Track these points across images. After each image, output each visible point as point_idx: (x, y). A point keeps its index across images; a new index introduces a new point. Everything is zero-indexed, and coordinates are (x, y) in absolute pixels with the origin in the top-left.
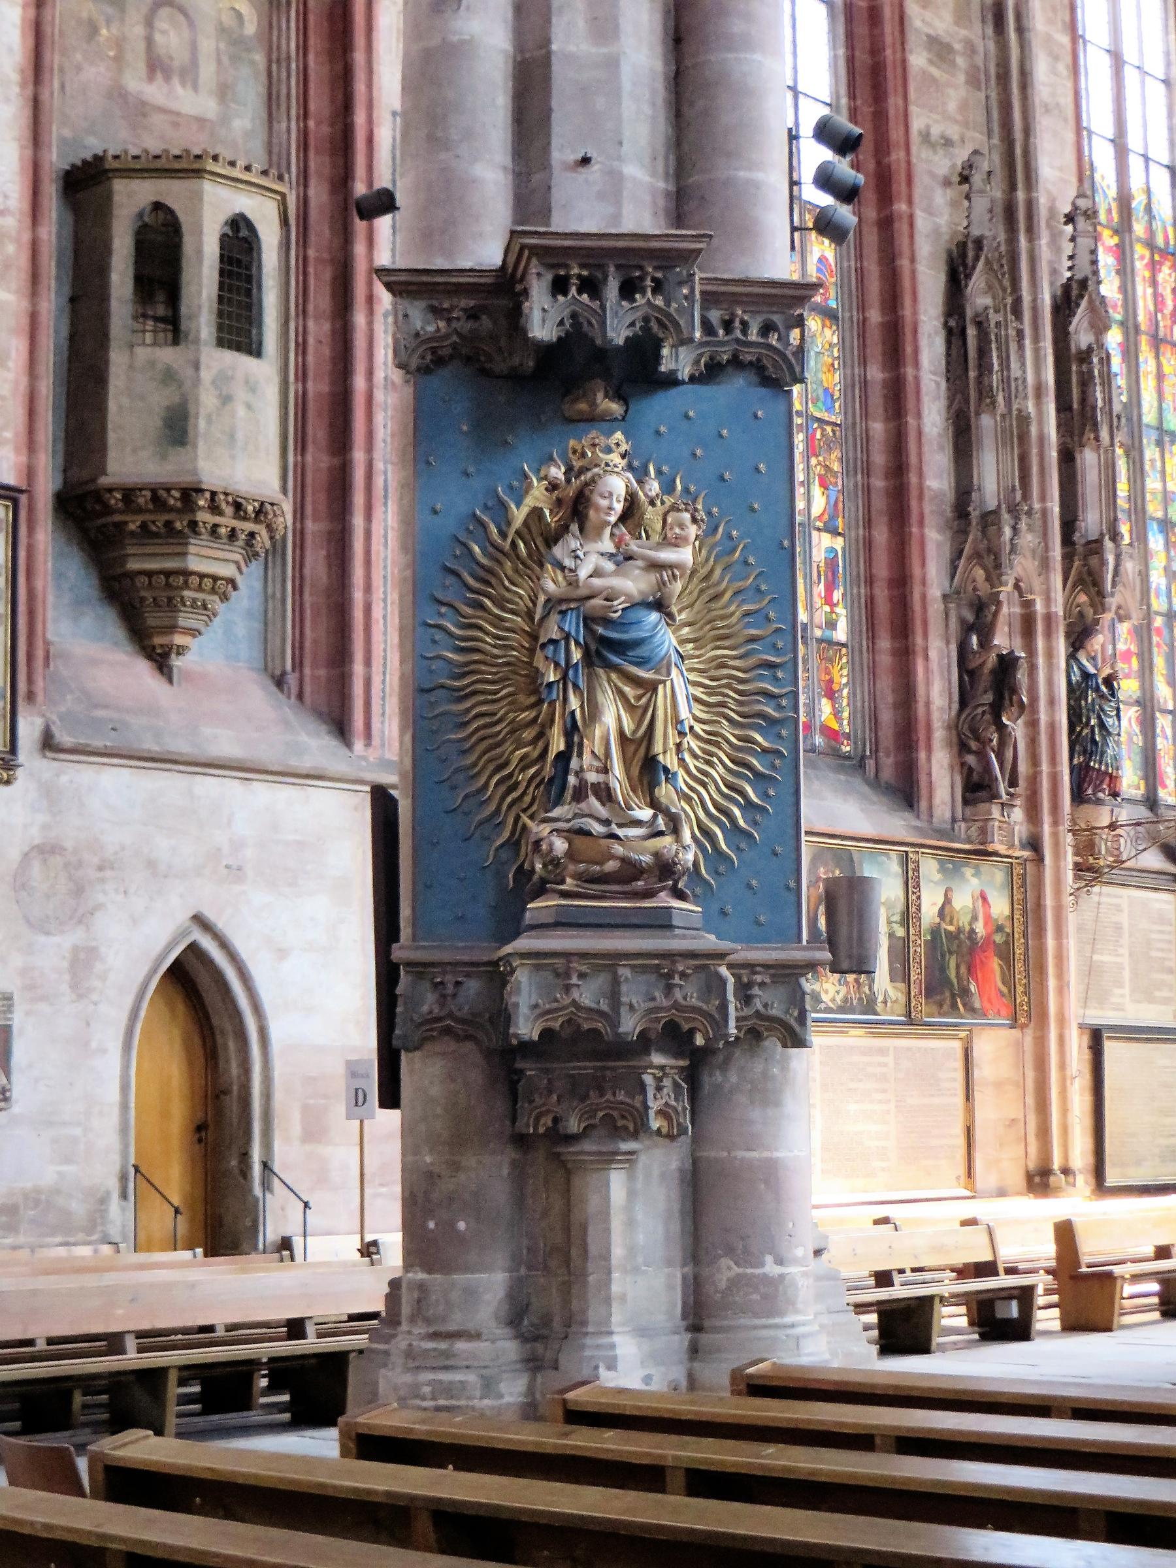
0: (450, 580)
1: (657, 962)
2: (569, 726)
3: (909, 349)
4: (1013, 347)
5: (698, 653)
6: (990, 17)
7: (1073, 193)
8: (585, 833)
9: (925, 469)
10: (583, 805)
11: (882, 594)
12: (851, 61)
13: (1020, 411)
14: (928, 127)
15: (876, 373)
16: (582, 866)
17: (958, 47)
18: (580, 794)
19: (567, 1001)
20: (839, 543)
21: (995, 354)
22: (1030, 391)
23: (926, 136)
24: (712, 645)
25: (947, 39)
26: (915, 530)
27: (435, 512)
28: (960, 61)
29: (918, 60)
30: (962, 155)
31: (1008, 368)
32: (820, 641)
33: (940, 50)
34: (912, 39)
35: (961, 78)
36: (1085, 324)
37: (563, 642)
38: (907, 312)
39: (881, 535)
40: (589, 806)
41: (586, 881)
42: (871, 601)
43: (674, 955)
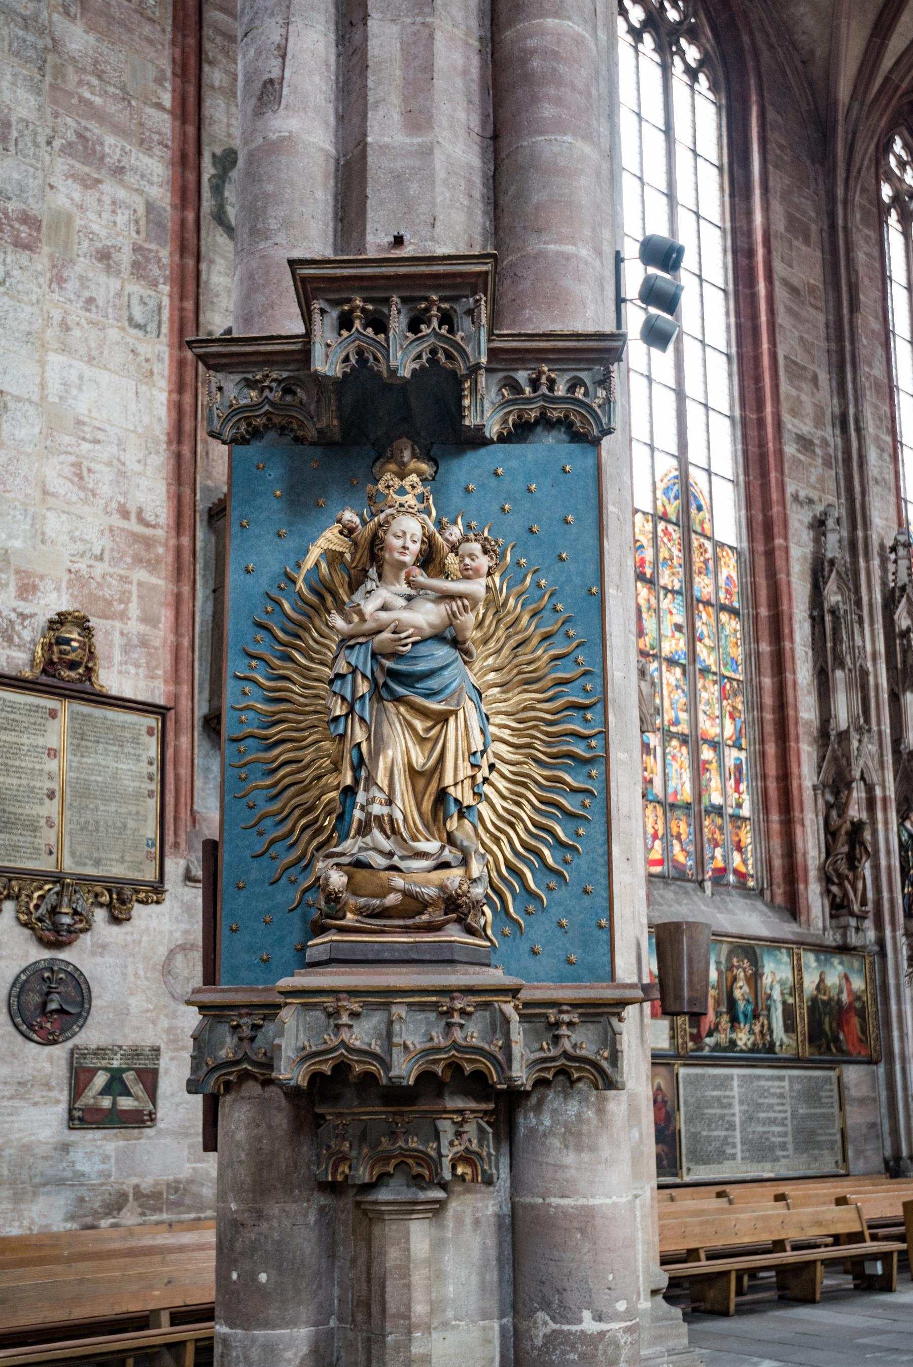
0: (261, 635)
1: (434, 999)
2: (355, 761)
3: (786, 631)
4: (856, 627)
6: (838, 423)
7: (894, 533)
8: (360, 864)
9: (799, 706)
10: (368, 839)
11: (772, 785)
12: (745, 452)
13: (861, 666)
14: (797, 491)
15: (765, 647)
16: (362, 901)
17: (817, 442)
18: (364, 829)
19: (335, 1042)
20: (743, 755)
21: (844, 631)
22: (869, 657)
23: (796, 498)
25: (808, 437)
26: (793, 744)
27: (248, 571)
28: (818, 451)
29: (790, 449)
30: (819, 508)
31: (853, 640)
32: (731, 816)
33: (805, 443)
34: (786, 437)
35: (820, 461)
36: (905, 614)
37: (350, 677)
38: (785, 607)
39: (771, 749)
40: (373, 840)
41: (368, 916)
42: (765, 791)
43: (452, 991)
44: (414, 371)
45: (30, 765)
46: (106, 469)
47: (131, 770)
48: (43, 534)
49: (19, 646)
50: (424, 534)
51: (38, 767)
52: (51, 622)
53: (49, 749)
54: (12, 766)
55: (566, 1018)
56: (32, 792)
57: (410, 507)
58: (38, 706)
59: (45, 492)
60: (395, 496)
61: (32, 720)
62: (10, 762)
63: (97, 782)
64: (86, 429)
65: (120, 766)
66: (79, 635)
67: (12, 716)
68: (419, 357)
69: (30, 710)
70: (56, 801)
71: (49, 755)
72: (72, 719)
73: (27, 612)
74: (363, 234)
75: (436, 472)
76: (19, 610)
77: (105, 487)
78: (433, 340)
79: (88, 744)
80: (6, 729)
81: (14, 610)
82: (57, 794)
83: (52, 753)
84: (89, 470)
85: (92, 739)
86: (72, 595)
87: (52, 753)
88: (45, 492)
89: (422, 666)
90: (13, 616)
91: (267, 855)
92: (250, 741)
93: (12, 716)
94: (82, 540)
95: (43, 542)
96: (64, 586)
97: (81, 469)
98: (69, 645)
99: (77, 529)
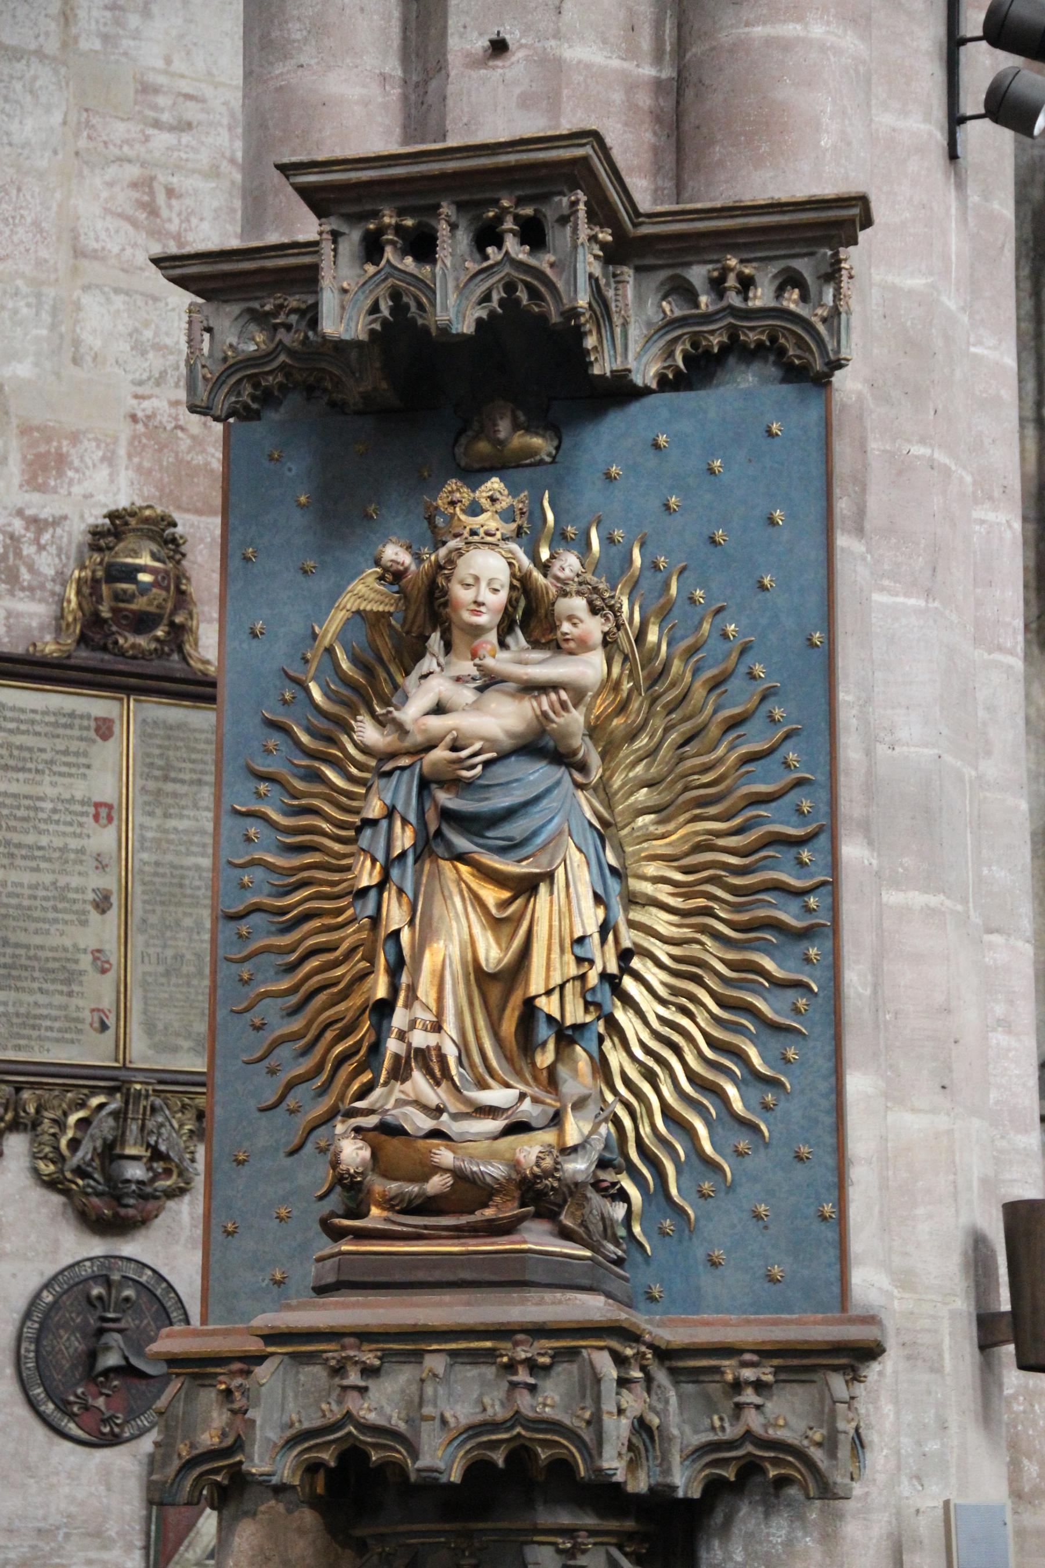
5: (661, 829)
24: (687, 816)
44: (479, 321)
45: (58, 842)
46: (205, 186)
48: (76, 343)
49: (31, 589)
50: (513, 575)
51: (74, 843)
52: (96, 533)
53: (97, 805)
54: (19, 846)
55: (748, 1374)
56: (64, 899)
57: (488, 534)
58: (72, 715)
59: (78, 252)
60: (463, 517)
62: (16, 838)
64: (162, 101)
66: (154, 557)
67: (18, 740)
68: (486, 298)
69: (56, 724)
70: (114, 914)
71: (96, 817)
72: (145, 736)
73: (45, 514)
74: (443, 35)
75: (558, 448)
76: (29, 512)
77: (206, 226)
78: (507, 269)
80: (6, 768)
81: (20, 513)
82: (114, 899)
83: (104, 813)
84: (170, 192)
85: (187, 776)
86: (139, 469)
87: (103, 812)
88: (78, 252)
89: (501, 801)
91: (284, 1105)
92: (256, 918)
93: (18, 740)
94: (157, 347)
95: (76, 361)
96: (122, 452)
97: (152, 193)
98: (134, 580)
99: (147, 324)
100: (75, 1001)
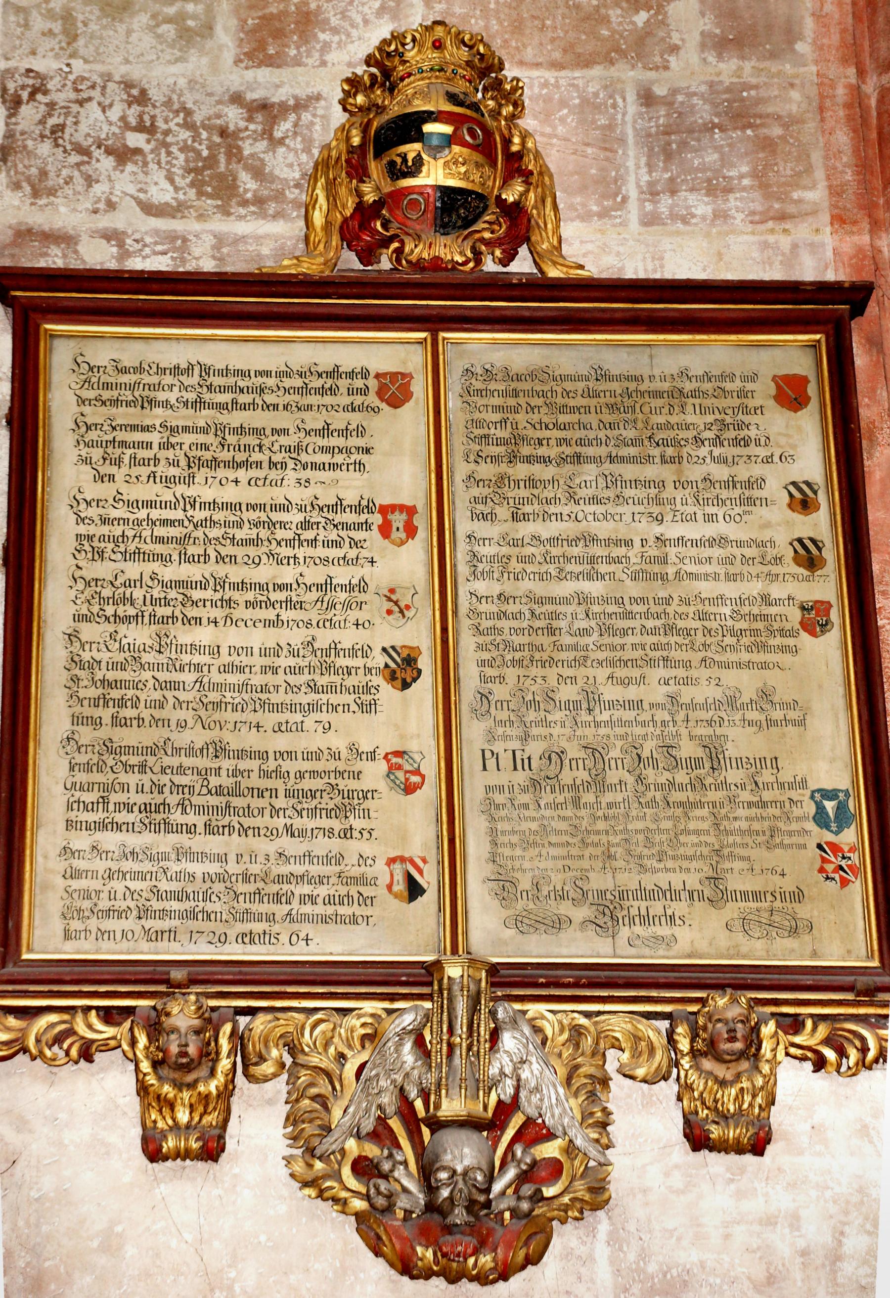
47: (722, 541)
49: (259, 201)
51: (342, 575)
53: (385, 510)
54: (241, 586)
56: (329, 668)
58: (335, 373)
61: (314, 421)
62: (235, 574)
63: (583, 599)
65: (673, 531)
67: (236, 418)
69: (304, 390)
71: (385, 530)
76: (250, 96)
79: (538, 471)
80: (215, 463)
81: (237, 99)
82: (425, 663)
85: (553, 452)
87: (398, 520)
90: (234, 116)
93: (236, 418)
100: (354, 847)
